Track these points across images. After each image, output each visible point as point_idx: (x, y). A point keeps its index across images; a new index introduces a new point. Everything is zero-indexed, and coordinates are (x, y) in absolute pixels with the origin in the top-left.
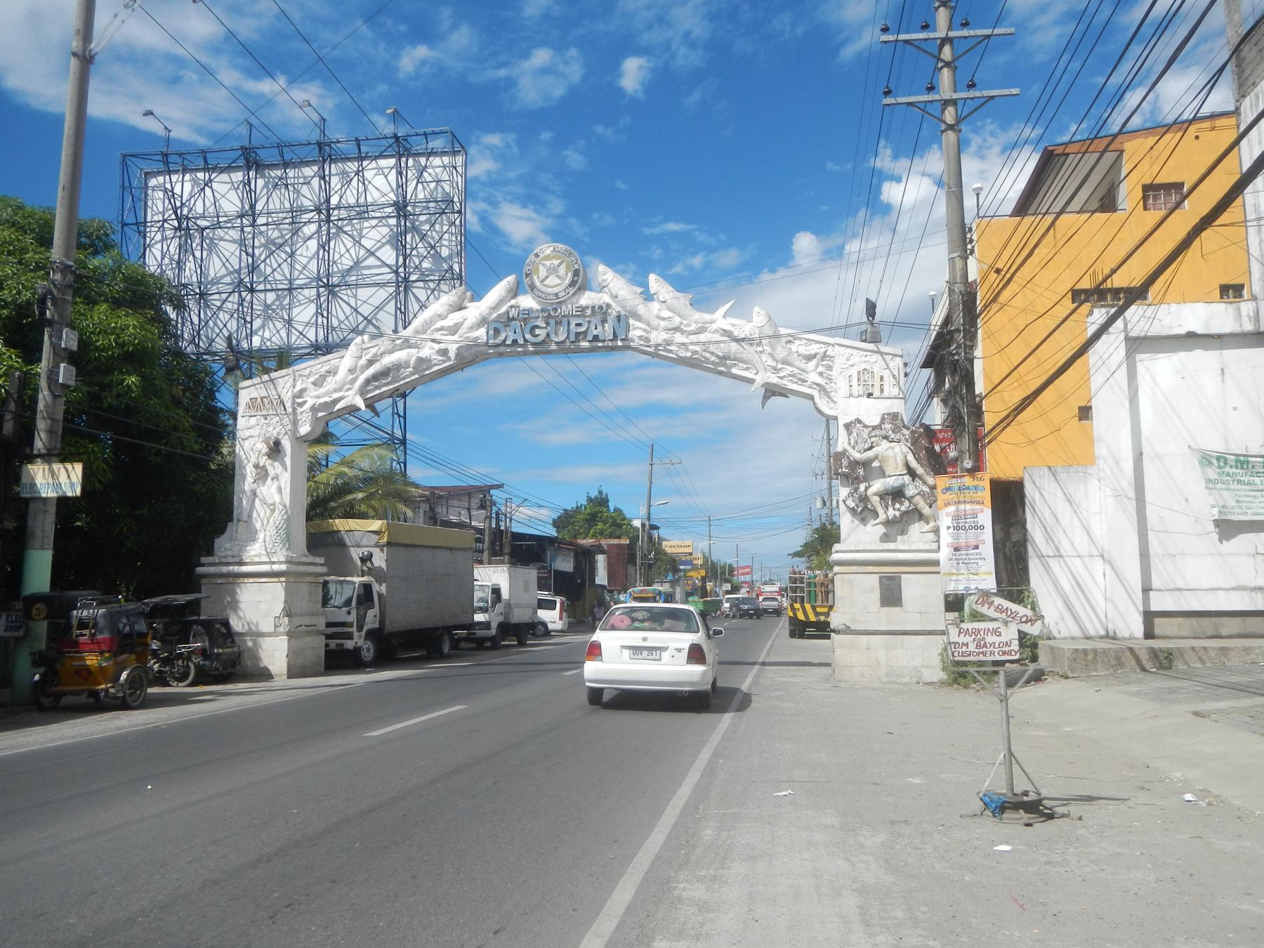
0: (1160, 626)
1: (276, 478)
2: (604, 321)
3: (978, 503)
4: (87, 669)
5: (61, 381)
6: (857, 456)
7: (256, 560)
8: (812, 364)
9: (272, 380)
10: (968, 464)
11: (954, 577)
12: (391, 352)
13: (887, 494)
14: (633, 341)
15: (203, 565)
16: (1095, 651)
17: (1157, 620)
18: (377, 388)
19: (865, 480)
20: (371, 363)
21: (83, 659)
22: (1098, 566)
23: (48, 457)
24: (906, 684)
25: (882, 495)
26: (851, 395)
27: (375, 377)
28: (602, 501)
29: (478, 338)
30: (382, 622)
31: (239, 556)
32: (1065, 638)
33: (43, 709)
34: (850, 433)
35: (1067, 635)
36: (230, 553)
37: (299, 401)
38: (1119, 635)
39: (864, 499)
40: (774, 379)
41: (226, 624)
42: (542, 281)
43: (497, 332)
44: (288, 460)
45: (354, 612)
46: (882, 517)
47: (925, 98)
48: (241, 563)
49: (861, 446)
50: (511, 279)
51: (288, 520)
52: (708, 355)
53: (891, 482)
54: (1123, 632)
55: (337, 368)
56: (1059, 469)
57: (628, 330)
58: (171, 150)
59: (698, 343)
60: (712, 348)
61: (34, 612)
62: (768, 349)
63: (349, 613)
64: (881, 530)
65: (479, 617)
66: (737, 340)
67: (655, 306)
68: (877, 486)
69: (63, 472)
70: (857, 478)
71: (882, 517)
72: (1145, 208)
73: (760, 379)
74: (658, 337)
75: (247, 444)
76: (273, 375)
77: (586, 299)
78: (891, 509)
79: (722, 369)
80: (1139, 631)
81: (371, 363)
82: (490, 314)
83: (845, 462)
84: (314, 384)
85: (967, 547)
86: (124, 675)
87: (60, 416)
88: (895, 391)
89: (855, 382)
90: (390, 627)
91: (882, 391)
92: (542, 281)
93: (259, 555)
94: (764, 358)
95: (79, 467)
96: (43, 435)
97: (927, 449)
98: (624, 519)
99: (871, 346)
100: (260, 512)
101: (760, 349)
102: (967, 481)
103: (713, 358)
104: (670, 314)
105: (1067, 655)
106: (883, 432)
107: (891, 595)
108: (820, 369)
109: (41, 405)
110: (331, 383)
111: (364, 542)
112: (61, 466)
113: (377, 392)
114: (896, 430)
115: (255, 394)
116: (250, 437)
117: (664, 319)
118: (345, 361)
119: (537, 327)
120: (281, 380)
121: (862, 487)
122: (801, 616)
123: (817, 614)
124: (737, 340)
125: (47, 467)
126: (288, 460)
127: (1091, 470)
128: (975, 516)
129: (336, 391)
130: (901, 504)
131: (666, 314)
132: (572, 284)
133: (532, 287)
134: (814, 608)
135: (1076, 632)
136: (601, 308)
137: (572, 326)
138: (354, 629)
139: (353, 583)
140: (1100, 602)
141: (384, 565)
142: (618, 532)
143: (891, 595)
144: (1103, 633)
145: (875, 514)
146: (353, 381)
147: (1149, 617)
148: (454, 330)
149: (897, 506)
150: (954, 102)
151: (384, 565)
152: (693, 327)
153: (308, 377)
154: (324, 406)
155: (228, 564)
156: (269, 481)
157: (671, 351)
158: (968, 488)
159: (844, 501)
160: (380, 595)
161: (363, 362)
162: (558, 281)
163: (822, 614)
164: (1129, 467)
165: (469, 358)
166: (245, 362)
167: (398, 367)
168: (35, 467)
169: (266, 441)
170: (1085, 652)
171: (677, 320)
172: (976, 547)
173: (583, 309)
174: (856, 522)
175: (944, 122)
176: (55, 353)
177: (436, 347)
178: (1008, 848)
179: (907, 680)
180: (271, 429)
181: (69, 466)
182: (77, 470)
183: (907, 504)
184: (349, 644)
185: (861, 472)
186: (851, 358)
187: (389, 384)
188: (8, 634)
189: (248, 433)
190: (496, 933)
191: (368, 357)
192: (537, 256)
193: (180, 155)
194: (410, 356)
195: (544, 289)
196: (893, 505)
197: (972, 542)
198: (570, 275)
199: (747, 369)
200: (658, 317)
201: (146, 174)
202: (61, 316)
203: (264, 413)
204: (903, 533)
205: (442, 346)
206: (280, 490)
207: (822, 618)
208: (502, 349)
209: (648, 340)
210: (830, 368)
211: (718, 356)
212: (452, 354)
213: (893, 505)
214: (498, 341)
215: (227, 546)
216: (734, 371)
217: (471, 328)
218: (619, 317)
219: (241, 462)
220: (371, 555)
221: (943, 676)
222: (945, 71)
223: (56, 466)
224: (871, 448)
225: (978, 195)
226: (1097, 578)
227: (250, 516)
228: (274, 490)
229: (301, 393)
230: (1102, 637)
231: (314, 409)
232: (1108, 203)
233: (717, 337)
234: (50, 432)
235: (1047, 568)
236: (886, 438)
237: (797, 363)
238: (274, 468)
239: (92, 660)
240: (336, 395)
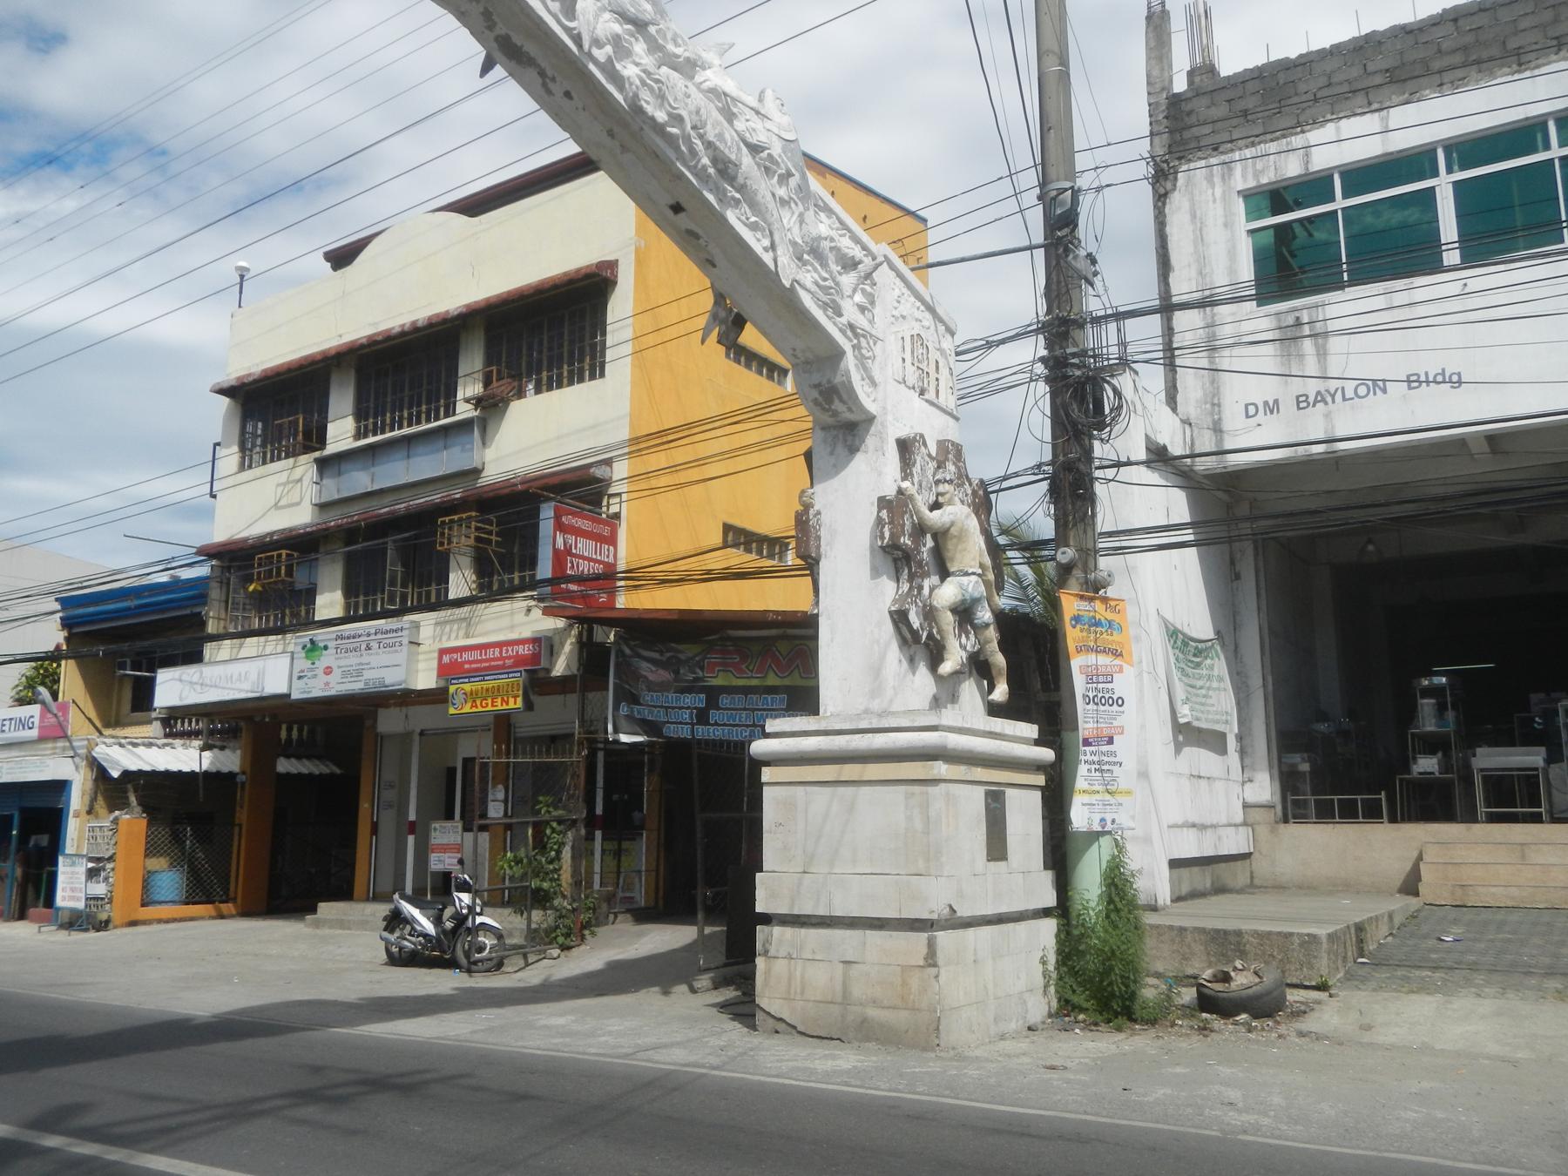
8: (848, 280)
39: (930, 614)
101: (782, 192)
108: (858, 298)
199: (754, 227)
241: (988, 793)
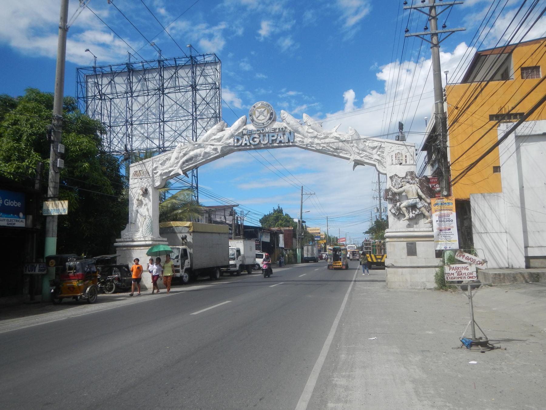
0: (533, 263)
1: (146, 205)
2: (284, 134)
3: (450, 210)
4: (73, 287)
5: (58, 166)
6: (395, 190)
7: (139, 239)
8: (375, 151)
9: (143, 163)
10: (445, 193)
11: (440, 243)
12: (193, 150)
13: (409, 207)
14: (296, 142)
15: (117, 242)
16: (504, 274)
17: (531, 260)
18: (187, 165)
19: (399, 201)
20: (185, 155)
21: (71, 283)
22: (504, 236)
23: (54, 198)
24: (419, 289)
25: (407, 207)
26: (392, 164)
27: (187, 161)
28: (280, 211)
29: (230, 143)
30: (191, 265)
31: (132, 238)
32: (490, 269)
33: (55, 304)
34: (392, 181)
35: (491, 267)
36: (128, 237)
37: (155, 172)
38: (515, 266)
39: (399, 209)
40: (358, 158)
41: (127, 267)
42: (257, 118)
43: (238, 140)
44: (151, 197)
45: (180, 261)
46: (407, 217)
47: (424, 33)
48: (133, 241)
49: (397, 186)
50: (243, 117)
51: (152, 222)
52: (329, 148)
53: (411, 201)
54: (516, 265)
55: (171, 157)
56: (486, 194)
57: (294, 138)
58: (97, 65)
59: (325, 143)
60: (331, 145)
61: (50, 263)
62: (356, 145)
63: (178, 261)
64: (407, 222)
65: (232, 262)
66: (342, 141)
67: (306, 128)
68: (405, 203)
69: (60, 204)
70: (396, 200)
71: (407, 217)
72: (522, 78)
73: (352, 158)
74: (307, 141)
75: (134, 191)
76: (144, 161)
77: (276, 125)
78: (411, 213)
79: (336, 154)
80: (523, 265)
81: (185, 155)
82: (235, 133)
83: (390, 193)
84: (161, 164)
85: (445, 229)
86: (88, 289)
87: (58, 181)
88: (412, 162)
89: (394, 159)
90: (195, 267)
91: (406, 162)
92: (257, 118)
93: (140, 238)
94: (354, 149)
95: (66, 202)
96: (51, 189)
97: (427, 187)
98: (290, 218)
99: (401, 143)
100: (140, 219)
101: (352, 145)
102: (445, 200)
103: (332, 149)
104: (312, 131)
105: (492, 276)
106: (407, 180)
107: (412, 251)
108: (378, 153)
109: (50, 177)
110: (168, 164)
111: (183, 231)
112: (59, 202)
113: (188, 167)
114: (413, 178)
115: (137, 169)
116: (135, 187)
117: (310, 133)
118: (174, 155)
119: (255, 138)
120: (147, 163)
121: (398, 204)
122: (370, 260)
123: (377, 259)
124: (342, 141)
125: (53, 202)
126: (151, 197)
127: (501, 195)
128: (448, 215)
129: (170, 167)
130: (416, 211)
131: (311, 131)
132: (270, 119)
133: (253, 120)
134: (375, 256)
135: (495, 266)
136: (282, 129)
137: (270, 136)
138: (180, 268)
139: (179, 249)
140: (505, 252)
141: (191, 241)
142: (288, 224)
143: (412, 251)
144: (507, 266)
145: (404, 216)
146: (178, 162)
147: (528, 259)
148: (219, 140)
149: (414, 212)
150: (436, 34)
151: (191, 241)
152: (323, 136)
153: (158, 161)
154: (166, 173)
155: (127, 241)
156: (143, 206)
157: (313, 147)
158: (445, 204)
159: (390, 210)
160: (190, 254)
161: (181, 154)
162: (264, 118)
163: (379, 259)
164: (518, 192)
165: (226, 152)
166: (131, 156)
167: (196, 156)
168: (49, 203)
169: (142, 189)
170: (499, 275)
171: (316, 133)
172: (449, 229)
173: (275, 129)
174: (396, 219)
175: (432, 43)
176: (55, 154)
177: (212, 147)
178: (475, 362)
179: (419, 287)
180: (143, 184)
181: (63, 202)
182: (66, 204)
183: (418, 211)
184: (178, 275)
185: (398, 197)
186: (392, 148)
187: (192, 163)
188: (40, 273)
189: (134, 186)
190: (261, 400)
191: (184, 152)
192: (254, 107)
193: (101, 67)
194: (201, 151)
195: (258, 121)
196: (412, 211)
197: (448, 227)
198: (269, 115)
199: (346, 154)
200: (307, 132)
201: (87, 76)
202: (58, 139)
203: (141, 177)
204: (416, 224)
205: (215, 147)
206: (148, 210)
207: (379, 261)
208: (240, 148)
209: (303, 142)
210: (383, 152)
211: (334, 149)
212: (219, 150)
213: (412, 211)
214: (238, 144)
215: (127, 234)
216: (341, 155)
217: (227, 139)
218: (290, 133)
219: (131, 198)
220: (186, 237)
221: (435, 285)
222: (433, 21)
223: (57, 202)
224: (402, 187)
225: (446, 74)
226: (503, 241)
227: (135, 221)
228: (145, 210)
229: (156, 168)
230: (507, 268)
231: (161, 175)
232: (505, 76)
233: (333, 140)
234: (54, 188)
235: (481, 237)
236: (408, 182)
237: (368, 151)
238: (145, 201)
239: (75, 283)
240: (170, 169)
241: (407, 243)
